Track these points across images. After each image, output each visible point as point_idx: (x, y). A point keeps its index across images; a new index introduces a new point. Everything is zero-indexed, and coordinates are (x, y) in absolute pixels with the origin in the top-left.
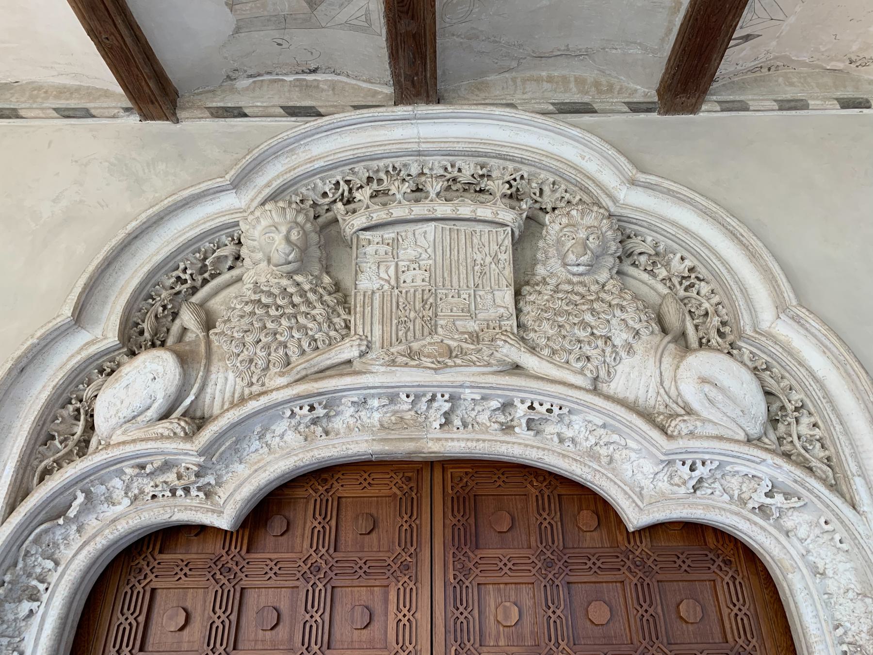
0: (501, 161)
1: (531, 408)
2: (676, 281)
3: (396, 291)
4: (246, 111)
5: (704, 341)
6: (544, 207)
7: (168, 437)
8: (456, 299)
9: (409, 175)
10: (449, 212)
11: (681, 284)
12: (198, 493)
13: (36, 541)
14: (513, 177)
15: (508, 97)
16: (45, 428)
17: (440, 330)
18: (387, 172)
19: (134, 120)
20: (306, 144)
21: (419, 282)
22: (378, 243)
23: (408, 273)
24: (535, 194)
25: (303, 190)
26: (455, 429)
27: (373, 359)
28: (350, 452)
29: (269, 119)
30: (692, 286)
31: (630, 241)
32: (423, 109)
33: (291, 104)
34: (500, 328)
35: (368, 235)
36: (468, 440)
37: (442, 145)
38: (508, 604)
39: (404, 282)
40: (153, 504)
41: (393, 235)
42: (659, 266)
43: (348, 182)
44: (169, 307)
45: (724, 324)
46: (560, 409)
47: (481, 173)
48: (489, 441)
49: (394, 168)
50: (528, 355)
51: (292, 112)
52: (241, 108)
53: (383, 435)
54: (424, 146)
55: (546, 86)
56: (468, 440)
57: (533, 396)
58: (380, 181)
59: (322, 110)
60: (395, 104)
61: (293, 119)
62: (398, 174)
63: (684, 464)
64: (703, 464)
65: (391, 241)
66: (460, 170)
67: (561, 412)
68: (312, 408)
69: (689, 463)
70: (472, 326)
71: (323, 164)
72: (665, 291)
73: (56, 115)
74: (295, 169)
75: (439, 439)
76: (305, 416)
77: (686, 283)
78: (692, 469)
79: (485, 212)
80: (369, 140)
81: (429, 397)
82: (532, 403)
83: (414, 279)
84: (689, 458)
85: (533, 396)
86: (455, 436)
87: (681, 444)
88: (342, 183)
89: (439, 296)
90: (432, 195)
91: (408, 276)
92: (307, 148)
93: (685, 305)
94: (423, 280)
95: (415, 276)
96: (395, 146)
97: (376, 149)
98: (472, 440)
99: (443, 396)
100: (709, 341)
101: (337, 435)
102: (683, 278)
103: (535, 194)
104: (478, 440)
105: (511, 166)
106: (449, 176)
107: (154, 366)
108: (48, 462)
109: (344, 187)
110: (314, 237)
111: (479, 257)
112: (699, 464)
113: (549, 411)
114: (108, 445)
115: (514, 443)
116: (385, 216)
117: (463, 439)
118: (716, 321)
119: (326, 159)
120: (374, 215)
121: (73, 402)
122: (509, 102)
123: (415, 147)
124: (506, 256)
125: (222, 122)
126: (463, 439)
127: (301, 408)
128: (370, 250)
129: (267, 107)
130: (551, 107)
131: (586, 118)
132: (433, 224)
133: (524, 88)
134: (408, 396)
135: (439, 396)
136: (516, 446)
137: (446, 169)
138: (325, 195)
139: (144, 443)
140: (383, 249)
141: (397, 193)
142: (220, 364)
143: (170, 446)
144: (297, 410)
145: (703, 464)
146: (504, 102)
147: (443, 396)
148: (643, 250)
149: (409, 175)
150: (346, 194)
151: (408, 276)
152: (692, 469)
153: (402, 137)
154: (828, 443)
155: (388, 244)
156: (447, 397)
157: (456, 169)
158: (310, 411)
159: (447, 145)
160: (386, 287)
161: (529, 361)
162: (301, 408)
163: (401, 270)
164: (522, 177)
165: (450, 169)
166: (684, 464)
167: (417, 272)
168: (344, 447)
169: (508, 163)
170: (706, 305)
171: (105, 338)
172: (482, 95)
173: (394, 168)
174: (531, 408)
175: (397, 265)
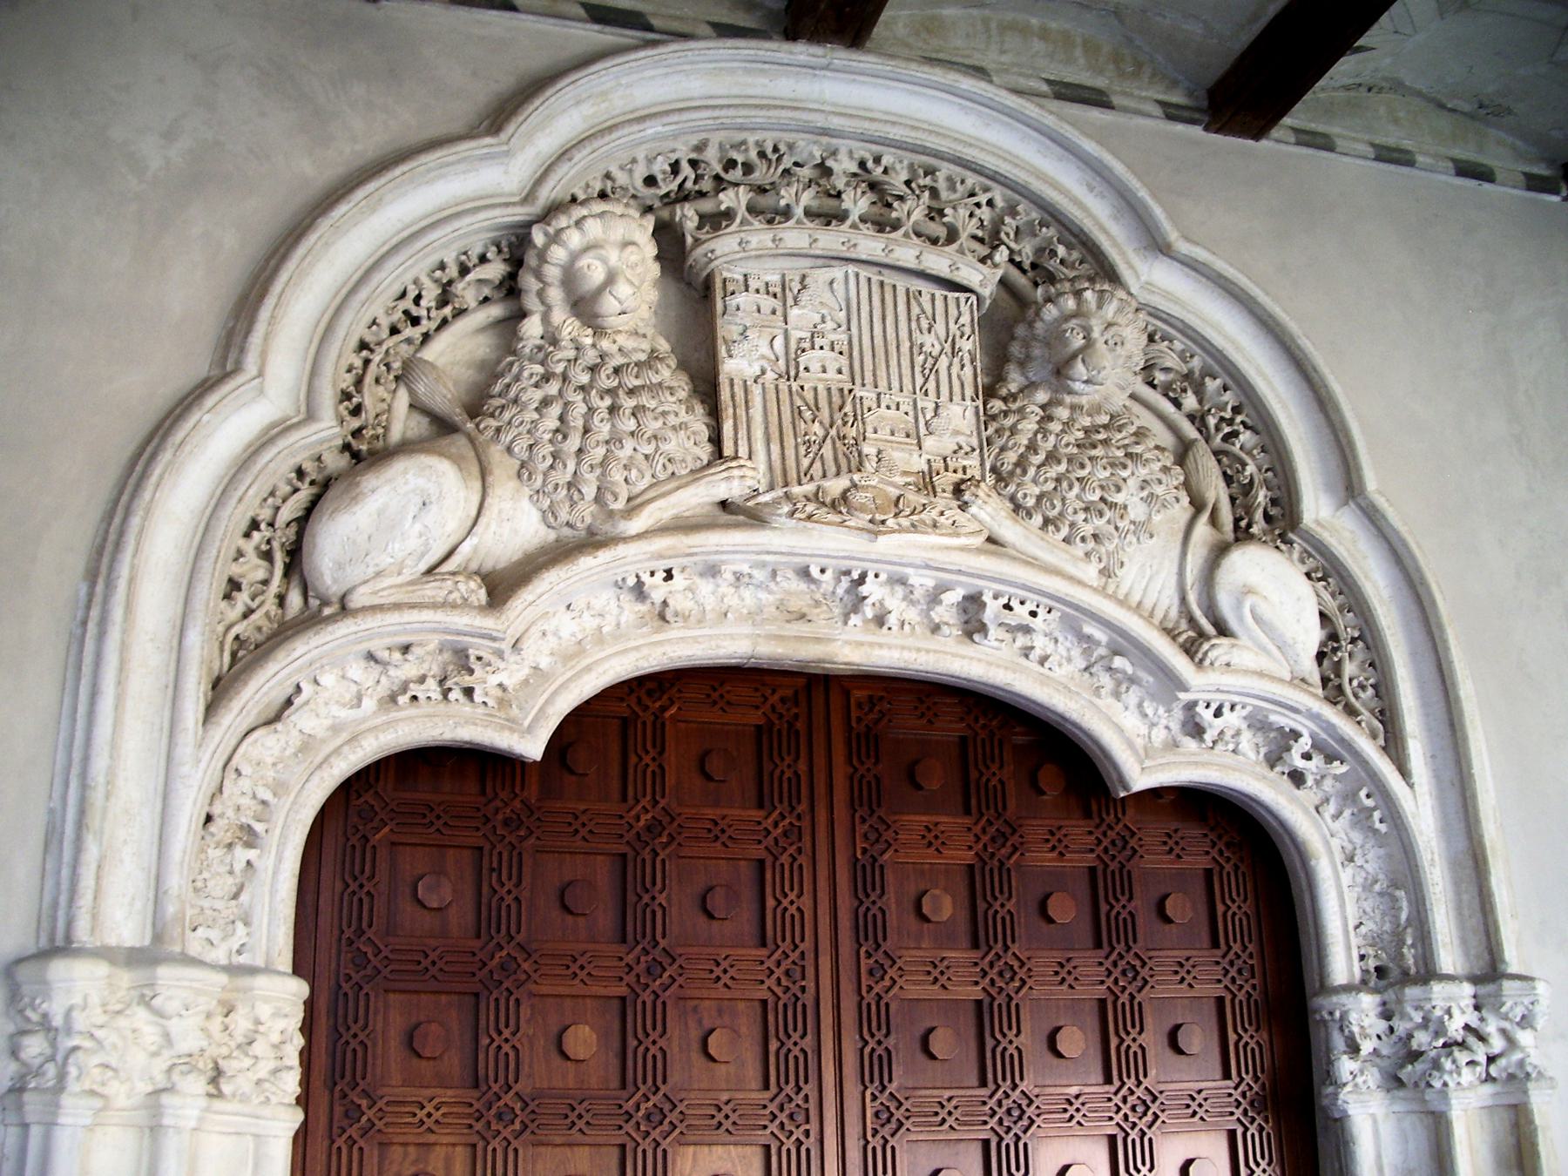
0: (958, 169)
2: (1212, 421)
5: (1243, 524)
6: (1018, 259)
7: (454, 606)
8: (892, 412)
9: (796, 164)
11: (1218, 429)
15: (977, 55)
18: (762, 155)
20: (629, 86)
21: (831, 374)
22: (758, 291)
23: (809, 354)
24: (1007, 234)
27: (766, 504)
28: (722, 652)
30: (1235, 434)
32: (840, 56)
34: (964, 469)
36: (903, 648)
37: (866, 125)
38: (937, 892)
39: (807, 369)
40: (412, 711)
42: (1190, 393)
43: (694, 163)
45: (1274, 502)
47: (922, 182)
49: (776, 149)
50: (1009, 523)
51: (602, 16)
54: (836, 122)
55: (1038, 45)
56: (903, 648)
57: (1012, 590)
58: (748, 168)
59: (655, 22)
60: (791, 35)
61: (597, 27)
62: (779, 159)
63: (1208, 706)
64: (1232, 708)
65: (778, 290)
67: (1049, 617)
68: (669, 575)
69: (1214, 706)
71: (660, 129)
72: (1191, 432)
74: (611, 129)
75: (861, 644)
76: (656, 587)
77: (1227, 430)
78: (1218, 713)
79: (938, 262)
80: (735, 91)
81: (855, 575)
84: (1216, 699)
89: (866, 404)
90: (854, 217)
91: (812, 359)
93: (1219, 461)
94: (840, 372)
96: (784, 113)
97: (753, 113)
98: (910, 649)
99: (876, 576)
100: (1249, 525)
102: (1222, 419)
103: (1007, 234)
105: (972, 180)
106: (866, 176)
107: (421, 482)
109: (686, 170)
111: (928, 340)
112: (1226, 710)
113: (1033, 614)
114: (344, 610)
117: (896, 647)
118: (1262, 496)
121: (263, 526)
122: (977, 63)
123: (820, 121)
124: (966, 345)
126: (896, 647)
127: (652, 574)
128: (741, 299)
130: (1045, 88)
131: (1095, 114)
133: (1002, 42)
134: (823, 571)
135: (871, 576)
137: (862, 164)
138: (650, 181)
139: (415, 611)
140: (767, 303)
141: (793, 204)
143: (462, 620)
145: (1232, 708)
146: (967, 61)
147: (876, 576)
148: (1168, 364)
149: (796, 164)
150: (689, 184)
151: (812, 359)
152: (1218, 713)
153: (792, 95)
154: (1383, 690)
155: (775, 296)
156: (883, 577)
157: (881, 169)
158: (666, 580)
159: (874, 126)
162: (652, 574)
163: (793, 346)
164: (990, 203)
165: (870, 164)
166: (1208, 706)
167: (826, 353)
168: (713, 643)
169: (969, 173)
170: (1251, 469)
171: (310, 416)
172: (935, 42)
173: (776, 149)
174: (1007, 607)
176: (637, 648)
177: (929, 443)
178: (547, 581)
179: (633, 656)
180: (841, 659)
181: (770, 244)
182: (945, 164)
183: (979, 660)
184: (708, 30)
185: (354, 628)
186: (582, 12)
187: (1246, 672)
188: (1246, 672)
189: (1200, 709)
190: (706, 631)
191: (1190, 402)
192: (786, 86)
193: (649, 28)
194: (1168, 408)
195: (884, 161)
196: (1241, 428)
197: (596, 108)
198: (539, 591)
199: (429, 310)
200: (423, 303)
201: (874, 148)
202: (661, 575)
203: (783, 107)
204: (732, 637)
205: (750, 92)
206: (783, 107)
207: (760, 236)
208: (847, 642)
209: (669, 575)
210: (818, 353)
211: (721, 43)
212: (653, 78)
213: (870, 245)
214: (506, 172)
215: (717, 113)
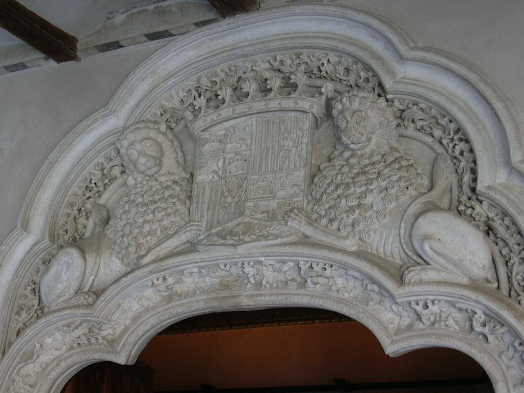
0: (310, 50)
1: (311, 267)
3: (223, 181)
4: (122, 43)
10: (263, 107)
12: (103, 341)
13: (18, 373)
14: (321, 62)
16: (16, 303)
17: (247, 212)
19: (52, 63)
24: (340, 74)
25: (164, 102)
26: (264, 287)
29: (139, 45)
31: (409, 110)
32: (240, 18)
33: (152, 31)
35: (206, 135)
36: (271, 295)
41: (223, 132)
44: (83, 209)
46: (332, 266)
48: (287, 294)
51: (152, 37)
52: (117, 42)
53: (212, 295)
57: (313, 260)
61: (156, 41)
66: (282, 62)
68: (165, 279)
70: (273, 204)
71: (174, 80)
73: (7, 71)
75: (252, 295)
78: (426, 307)
82: (311, 265)
83: (236, 168)
85: (313, 260)
86: (263, 292)
87: (408, 289)
88: (193, 90)
92: (164, 67)
95: (236, 166)
99: (249, 264)
101: (186, 296)
104: (278, 295)
108: (20, 325)
110: (166, 145)
115: (304, 295)
116: (216, 118)
117: (268, 295)
119: (176, 75)
120: (209, 119)
125: (108, 53)
126: (268, 295)
129: (135, 37)
132: (254, 118)
136: (305, 297)
139: (64, 311)
142: (109, 251)
144: (155, 282)
152: (426, 307)
160: (216, 178)
161: (309, 231)
162: (158, 280)
163: (227, 161)
167: (239, 162)
169: (316, 50)
174: (311, 267)
175: (225, 160)
176: (160, 312)
177: (280, 194)
178: (109, 291)
179: (157, 316)
180: (242, 304)
181: (216, 118)
182: (304, 50)
183: (307, 295)
184: (194, 27)
185: (45, 320)
186: (145, 38)
187: (429, 283)
188: (429, 283)
189: (414, 305)
190: (187, 300)
191: (438, 133)
192: (230, 40)
193: (172, 35)
194: (429, 140)
195: (278, 59)
196: (457, 142)
197: (152, 79)
198: (106, 295)
199: (95, 184)
200: (93, 181)
201: (272, 54)
202: (161, 280)
203: (224, 52)
204: (197, 301)
205: (215, 48)
206: (224, 52)
207: (212, 117)
208: (246, 296)
209: (165, 279)
210: (237, 163)
211: (200, 30)
212: (172, 58)
213: (260, 105)
214: (118, 119)
215: (196, 65)
